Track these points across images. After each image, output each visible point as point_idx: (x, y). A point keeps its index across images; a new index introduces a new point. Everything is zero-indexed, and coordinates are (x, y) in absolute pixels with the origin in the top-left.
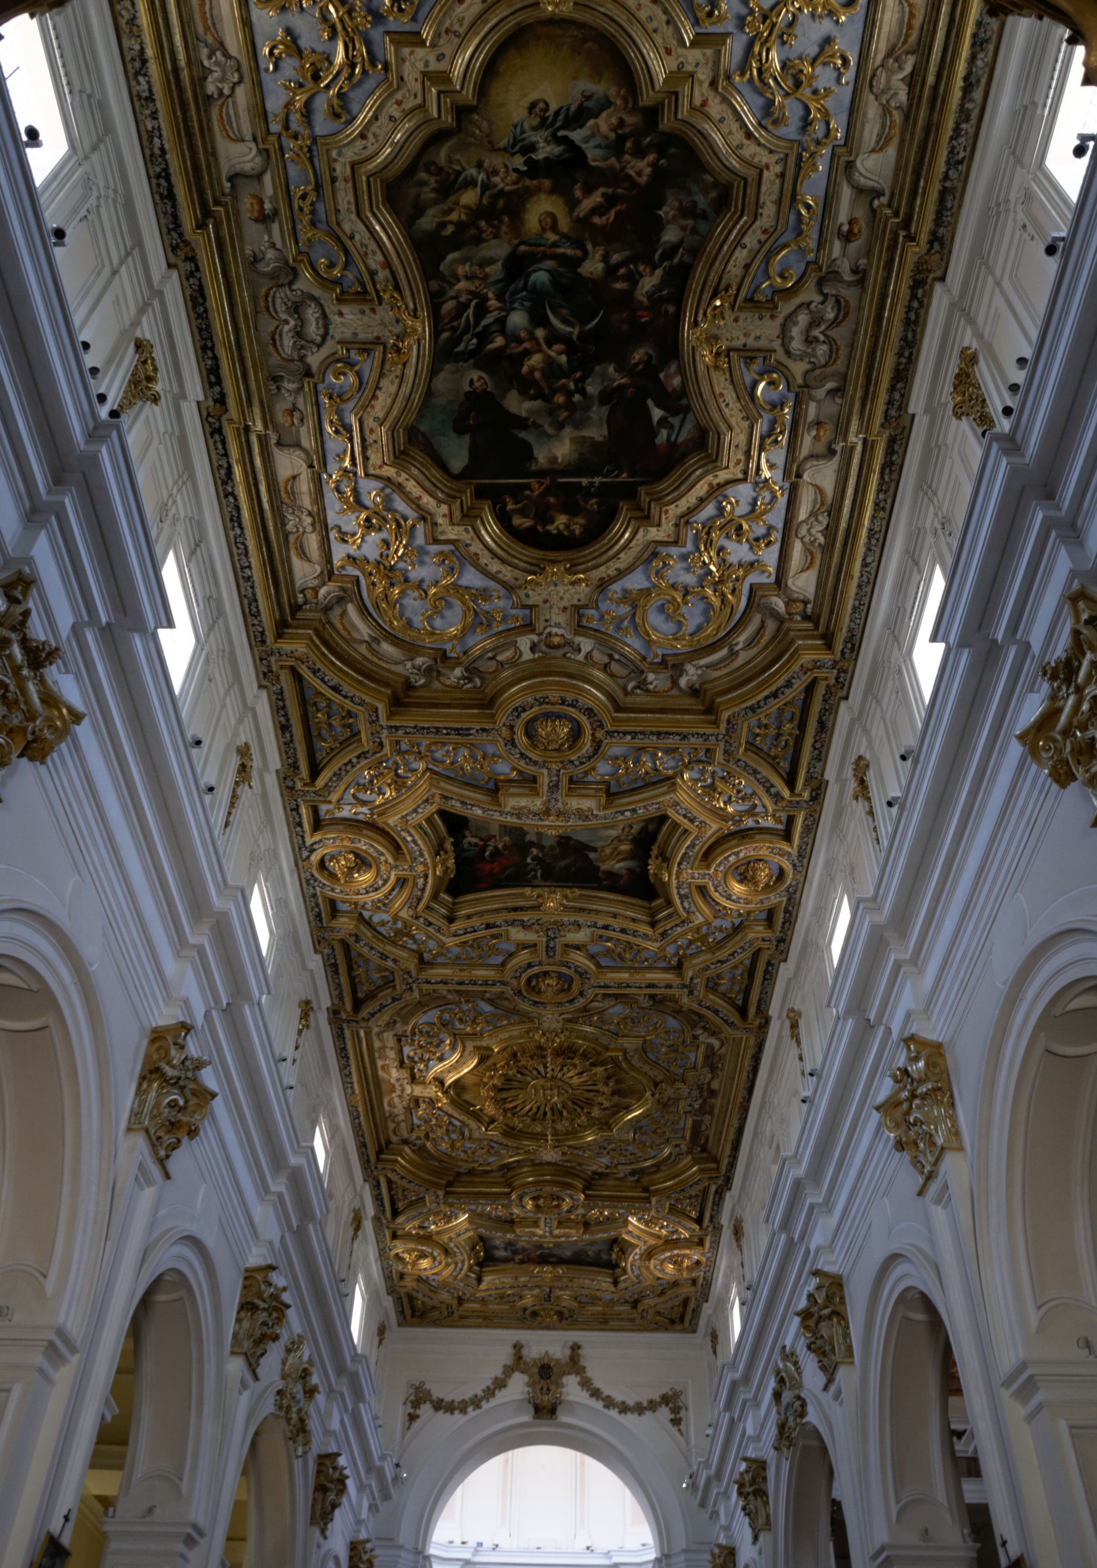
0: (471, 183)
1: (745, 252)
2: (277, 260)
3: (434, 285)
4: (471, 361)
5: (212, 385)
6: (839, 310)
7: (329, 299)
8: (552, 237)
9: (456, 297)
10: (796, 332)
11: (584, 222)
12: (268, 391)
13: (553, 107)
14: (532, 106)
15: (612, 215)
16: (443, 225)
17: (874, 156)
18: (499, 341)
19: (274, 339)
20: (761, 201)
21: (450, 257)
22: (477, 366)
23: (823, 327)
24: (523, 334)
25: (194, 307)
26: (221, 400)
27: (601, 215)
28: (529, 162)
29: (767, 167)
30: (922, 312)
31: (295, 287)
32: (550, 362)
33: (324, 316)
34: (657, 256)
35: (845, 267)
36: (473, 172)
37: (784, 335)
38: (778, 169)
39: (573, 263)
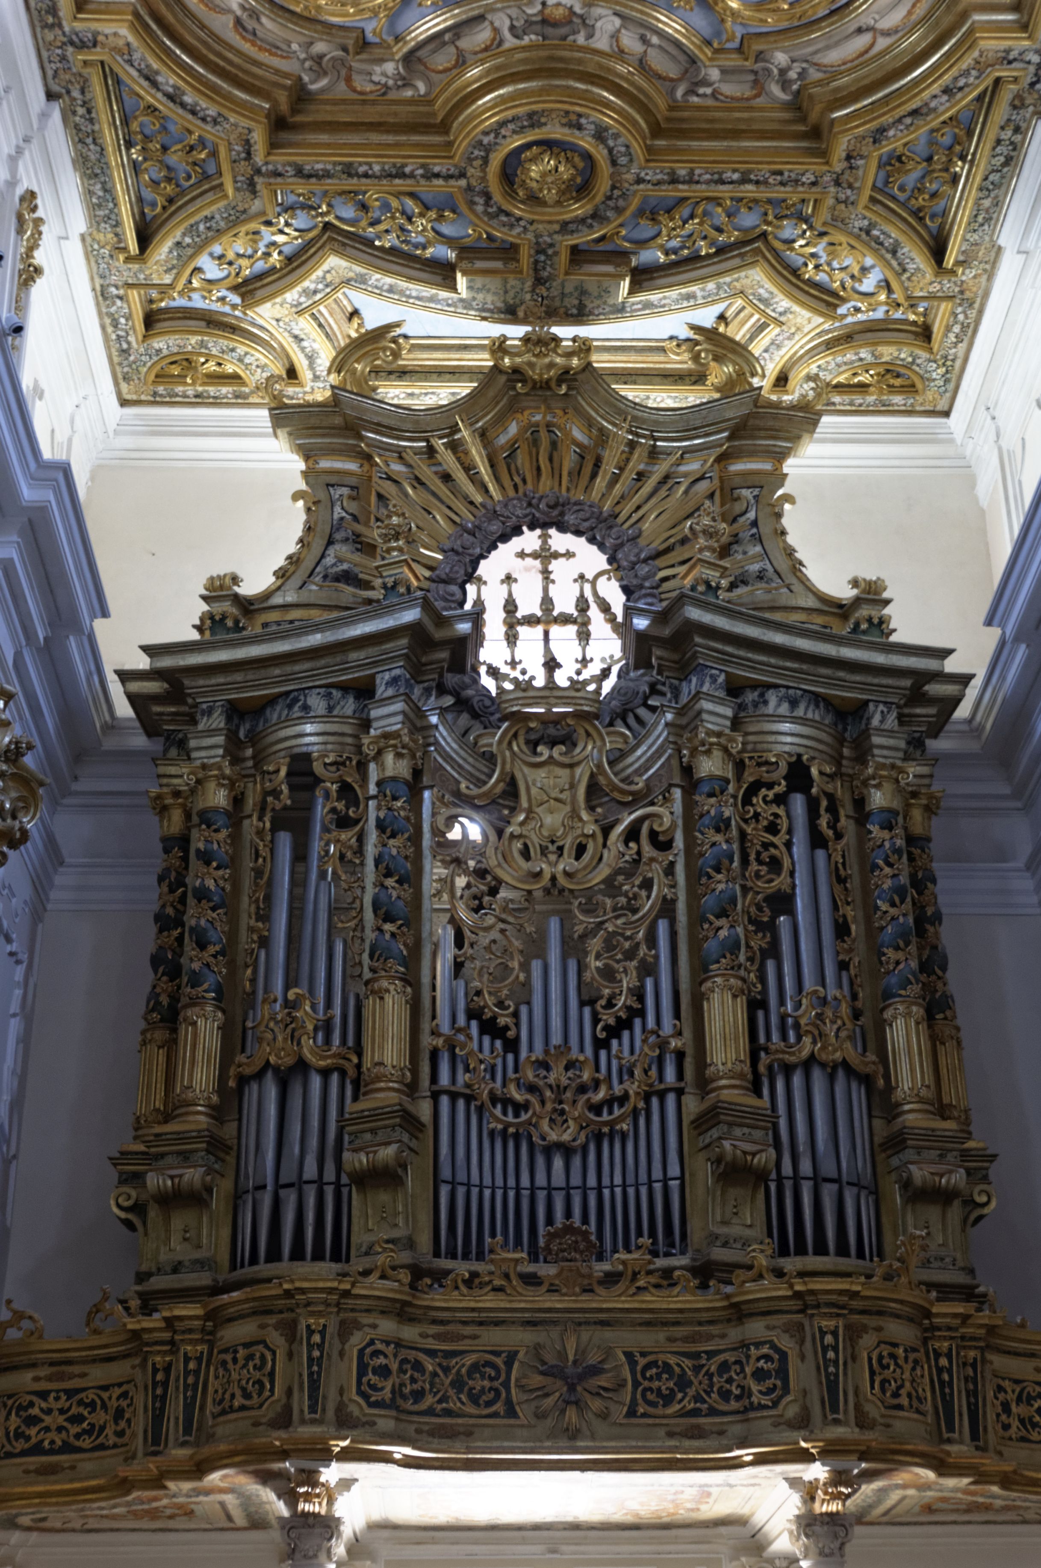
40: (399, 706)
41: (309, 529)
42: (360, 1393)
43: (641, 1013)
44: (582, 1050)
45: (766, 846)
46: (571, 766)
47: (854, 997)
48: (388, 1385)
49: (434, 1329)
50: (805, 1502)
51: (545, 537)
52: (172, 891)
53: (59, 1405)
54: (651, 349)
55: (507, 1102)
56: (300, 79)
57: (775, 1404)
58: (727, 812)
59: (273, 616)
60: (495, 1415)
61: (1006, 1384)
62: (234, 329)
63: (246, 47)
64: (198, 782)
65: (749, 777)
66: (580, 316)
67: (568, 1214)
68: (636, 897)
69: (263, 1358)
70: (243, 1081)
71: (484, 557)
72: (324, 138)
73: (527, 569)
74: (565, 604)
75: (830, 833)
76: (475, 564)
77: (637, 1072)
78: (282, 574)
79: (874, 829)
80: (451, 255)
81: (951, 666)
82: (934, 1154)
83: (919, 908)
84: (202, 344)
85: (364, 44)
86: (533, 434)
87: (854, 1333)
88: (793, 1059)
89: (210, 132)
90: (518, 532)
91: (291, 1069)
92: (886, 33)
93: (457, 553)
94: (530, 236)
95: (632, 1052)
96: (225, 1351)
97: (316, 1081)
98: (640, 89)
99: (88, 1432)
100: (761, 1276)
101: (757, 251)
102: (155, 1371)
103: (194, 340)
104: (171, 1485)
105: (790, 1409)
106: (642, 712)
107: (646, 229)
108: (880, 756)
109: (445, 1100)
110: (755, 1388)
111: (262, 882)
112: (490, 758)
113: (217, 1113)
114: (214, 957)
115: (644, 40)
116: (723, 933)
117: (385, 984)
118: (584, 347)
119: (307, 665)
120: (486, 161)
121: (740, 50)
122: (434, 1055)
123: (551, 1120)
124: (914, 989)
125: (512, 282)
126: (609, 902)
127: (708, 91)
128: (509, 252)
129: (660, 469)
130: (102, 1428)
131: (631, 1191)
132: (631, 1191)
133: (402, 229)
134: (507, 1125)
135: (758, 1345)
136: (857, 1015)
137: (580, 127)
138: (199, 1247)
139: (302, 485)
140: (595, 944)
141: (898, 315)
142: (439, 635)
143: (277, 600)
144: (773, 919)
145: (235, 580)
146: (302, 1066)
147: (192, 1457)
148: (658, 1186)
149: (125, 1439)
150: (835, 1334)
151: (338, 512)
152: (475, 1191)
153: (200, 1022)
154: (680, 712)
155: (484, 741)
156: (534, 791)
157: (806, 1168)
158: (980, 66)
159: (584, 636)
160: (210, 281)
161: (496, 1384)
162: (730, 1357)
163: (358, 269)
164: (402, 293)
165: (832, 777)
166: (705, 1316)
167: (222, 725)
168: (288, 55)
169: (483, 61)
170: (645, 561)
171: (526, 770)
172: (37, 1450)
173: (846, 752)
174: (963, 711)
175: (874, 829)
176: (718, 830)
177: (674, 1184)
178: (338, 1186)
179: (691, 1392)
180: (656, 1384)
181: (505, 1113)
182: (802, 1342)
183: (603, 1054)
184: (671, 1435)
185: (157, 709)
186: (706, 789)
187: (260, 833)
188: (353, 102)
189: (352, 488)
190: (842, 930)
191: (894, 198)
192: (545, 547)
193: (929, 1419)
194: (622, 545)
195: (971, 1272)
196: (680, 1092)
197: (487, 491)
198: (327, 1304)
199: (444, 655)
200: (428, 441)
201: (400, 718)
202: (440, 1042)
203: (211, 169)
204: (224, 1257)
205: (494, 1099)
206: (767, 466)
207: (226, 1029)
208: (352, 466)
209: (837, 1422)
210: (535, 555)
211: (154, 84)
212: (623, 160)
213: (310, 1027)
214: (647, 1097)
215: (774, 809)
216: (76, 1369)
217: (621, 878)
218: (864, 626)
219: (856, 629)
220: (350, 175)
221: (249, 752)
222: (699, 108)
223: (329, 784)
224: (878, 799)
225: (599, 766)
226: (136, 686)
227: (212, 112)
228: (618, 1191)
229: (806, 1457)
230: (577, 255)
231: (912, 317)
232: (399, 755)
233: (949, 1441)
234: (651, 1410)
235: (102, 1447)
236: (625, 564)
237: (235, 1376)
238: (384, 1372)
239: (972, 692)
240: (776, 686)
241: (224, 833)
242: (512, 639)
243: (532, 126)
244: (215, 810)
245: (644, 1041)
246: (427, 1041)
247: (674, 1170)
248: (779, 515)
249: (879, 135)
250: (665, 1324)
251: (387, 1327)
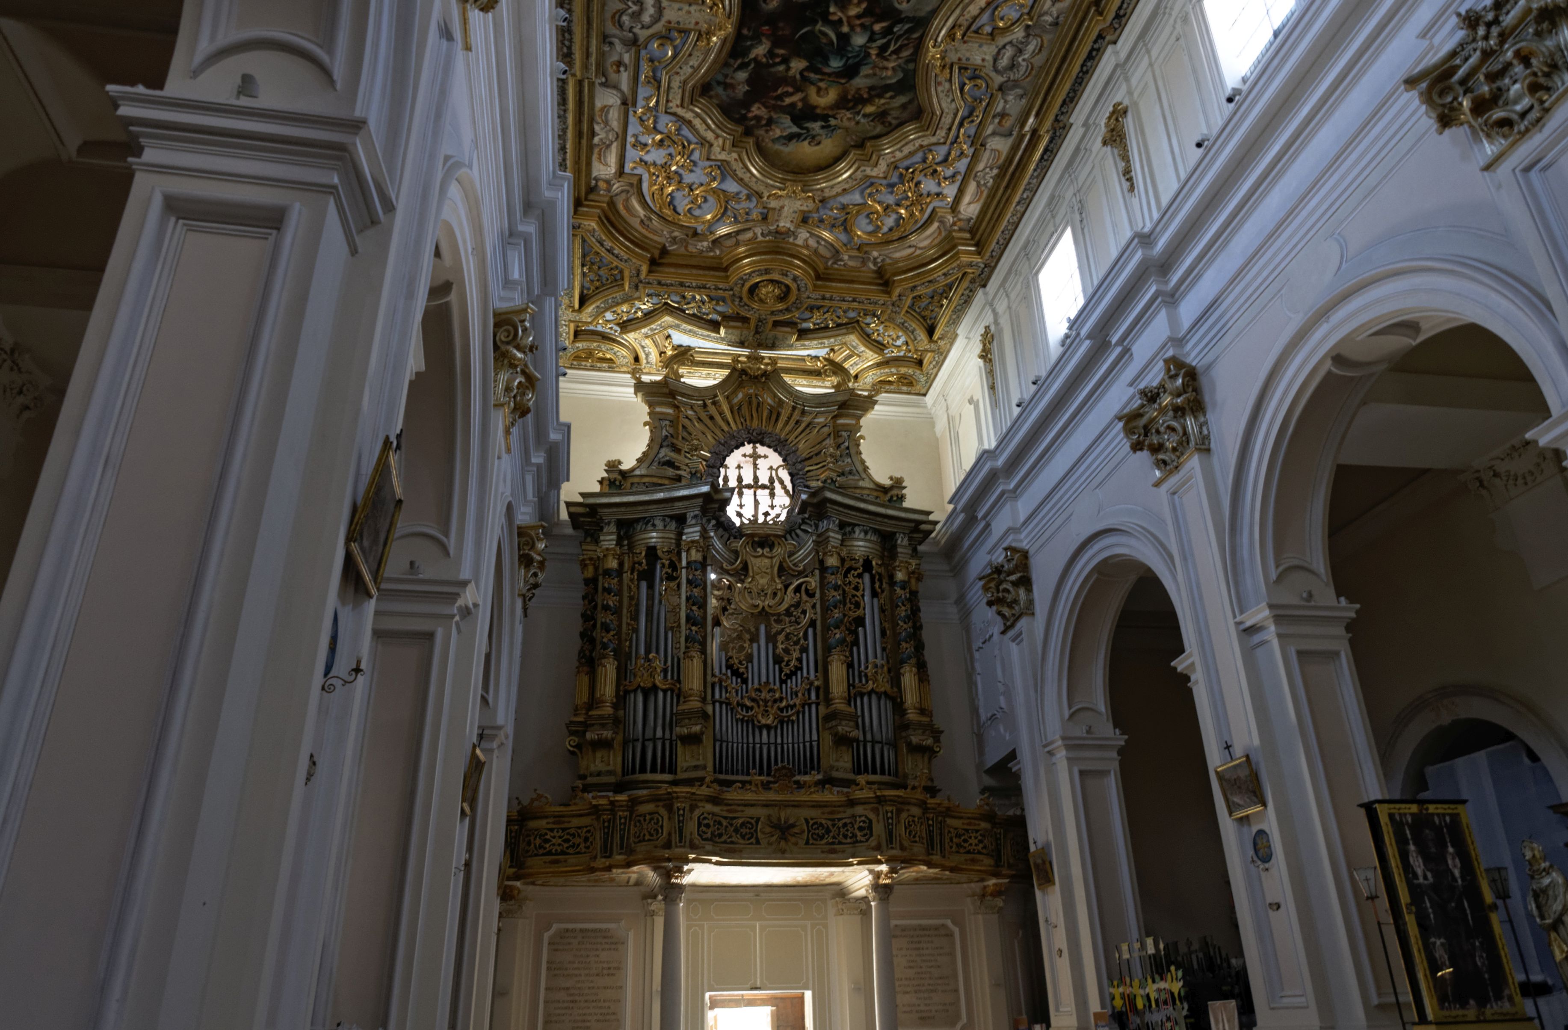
0: (865, 116)
1: (691, 63)
2: (1008, 95)
3: (911, 66)
4: (903, 16)
5: (1098, 50)
6: (619, 21)
7: (989, 70)
8: (822, 85)
9: (899, 58)
10: (651, 11)
11: (798, 90)
12: (1067, 18)
13: (806, 143)
14: (819, 143)
15: (780, 91)
16: (891, 98)
17: (610, 104)
18: (877, 27)
19: (1040, 50)
20: (680, 91)
21: (894, 81)
22: (900, 12)
23: (630, 11)
24: (858, 29)
25: (1074, 97)
26: (1100, 37)
27: (787, 92)
28: (827, 121)
29: (677, 106)
30: (560, 38)
31: (1005, 79)
32: (843, 7)
33: (995, 60)
34: (752, 65)
35: (619, 47)
36: (862, 121)
37: (660, 10)
38: (671, 104)
39: (811, 68)
40: (698, 528)
41: (652, 440)
42: (699, 835)
43: (801, 669)
44: (775, 684)
45: (854, 596)
46: (772, 558)
47: (888, 662)
48: (709, 831)
49: (725, 808)
50: (874, 878)
51: (754, 448)
52: (590, 603)
53: (559, 834)
54: (799, 360)
55: (743, 706)
56: (664, 246)
57: (867, 840)
58: (839, 583)
59: (636, 480)
60: (752, 844)
61: (952, 830)
62: (614, 341)
63: (644, 231)
64: (605, 556)
65: (847, 566)
66: (773, 347)
67: (782, 761)
68: (799, 617)
69: (658, 819)
70: (627, 692)
71: (728, 456)
72: (672, 270)
73: (747, 462)
74: (764, 480)
75: (879, 590)
76: (724, 459)
77: (800, 695)
78: (639, 460)
79: (898, 590)
80: (719, 318)
81: (932, 518)
82: (920, 732)
83: (914, 623)
84: (599, 346)
85: (695, 234)
86: (749, 399)
87: (899, 811)
88: (864, 691)
89: (622, 265)
90: (743, 445)
91: (650, 689)
92: (921, 248)
93: (717, 454)
94: (757, 315)
95: (797, 686)
96: (640, 816)
97: (661, 694)
98: (813, 261)
99: (573, 846)
100: (862, 789)
101: (854, 328)
102: (604, 822)
103: (595, 344)
104: (614, 871)
105: (873, 842)
106: (798, 531)
107: (807, 315)
108: (901, 557)
109: (717, 705)
110: (859, 834)
111: (634, 603)
112: (736, 553)
113: (615, 706)
114: (613, 636)
115: (818, 242)
116: (838, 636)
117: (694, 654)
118: (774, 361)
119: (655, 506)
120: (743, 285)
121: (858, 249)
122: (713, 686)
123: (763, 715)
124: (913, 661)
125: (745, 332)
126: (787, 619)
127: (842, 263)
128: (745, 320)
129: (806, 419)
130: (579, 845)
131: (796, 746)
132: (796, 746)
133: (699, 307)
134: (744, 716)
135: (860, 816)
136: (889, 671)
137: (787, 275)
138: (609, 764)
139: (647, 419)
140: (781, 638)
141: (910, 355)
142: (716, 497)
143: (637, 472)
144: (857, 628)
145: (620, 463)
146: (655, 688)
147: (625, 860)
148: (808, 744)
149: (590, 850)
150: (892, 812)
151: (664, 433)
152: (730, 744)
153: (608, 666)
154: (819, 536)
155: (734, 545)
156: (755, 568)
157: (869, 737)
158: (959, 267)
159: (772, 495)
160: (607, 321)
161: (752, 831)
162: (848, 821)
163: (677, 322)
164: (695, 333)
165: (880, 566)
166: (837, 804)
167: (615, 530)
168: (661, 236)
169: (747, 245)
170: (800, 462)
171: (752, 559)
172: (550, 853)
173: (886, 554)
174: (933, 535)
175: (898, 590)
176: (835, 590)
177: (815, 744)
178: (671, 740)
179: (831, 834)
180: (817, 831)
181: (742, 710)
182: (878, 815)
183: (784, 686)
184: (823, 852)
185: (582, 519)
186: (830, 571)
187: (632, 580)
188: (687, 256)
189: (671, 421)
190: (883, 633)
191: (915, 311)
192: (755, 452)
193: (926, 846)
194: (789, 454)
195: (932, 780)
196: (817, 704)
197: (729, 424)
198: (685, 798)
199: (716, 506)
200: (703, 400)
201: (698, 534)
202: (717, 680)
203: (618, 277)
204: (619, 770)
205: (738, 704)
206: (853, 422)
207: (618, 669)
208: (670, 411)
209: (892, 848)
210: (750, 456)
211: (602, 245)
212: (803, 289)
213: (659, 670)
215: (857, 580)
216: (566, 819)
217: (792, 609)
218: (895, 498)
219: (890, 500)
220: (682, 286)
221: (626, 542)
222: (837, 269)
223: (664, 561)
224: (900, 576)
225: (784, 558)
226: (573, 509)
227: (626, 257)
228: (790, 746)
229: (879, 862)
230: (776, 324)
231: (915, 356)
232: (698, 551)
233: (932, 854)
234: (815, 842)
235: (579, 853)
236: (790, 462)
237: (645, 827)
239: (938, 527)
240: (859, 525)
241: (616, 580)
243: (766, 274)
244: (611, 570)
245: (802, 682)
246: (709, 678)
247: (815, 737)
248: (859, 445)
249: (914, 288)
250: (820, 807)
251: (709, 807)
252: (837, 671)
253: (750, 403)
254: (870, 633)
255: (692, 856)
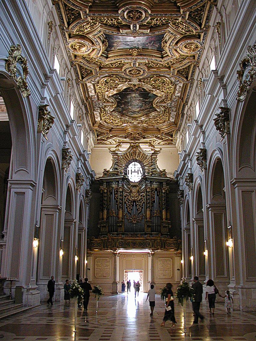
43: (142, 212)
59: (110, 173)
74: (136, 171)
87: (155, 241)
122: (124, 215)
140: (138, 205)
143: (110, 171)
175: (163, 194)
190: (159, 203)
206: (156, 156)
208: (117, 157)
214: (142, 219)
238: (120, 243)
242: (131, 174)
251: (121, 240)
252: (148, 212)
253: (134, 153)
254: (156, 205)
255: (117, 249)
